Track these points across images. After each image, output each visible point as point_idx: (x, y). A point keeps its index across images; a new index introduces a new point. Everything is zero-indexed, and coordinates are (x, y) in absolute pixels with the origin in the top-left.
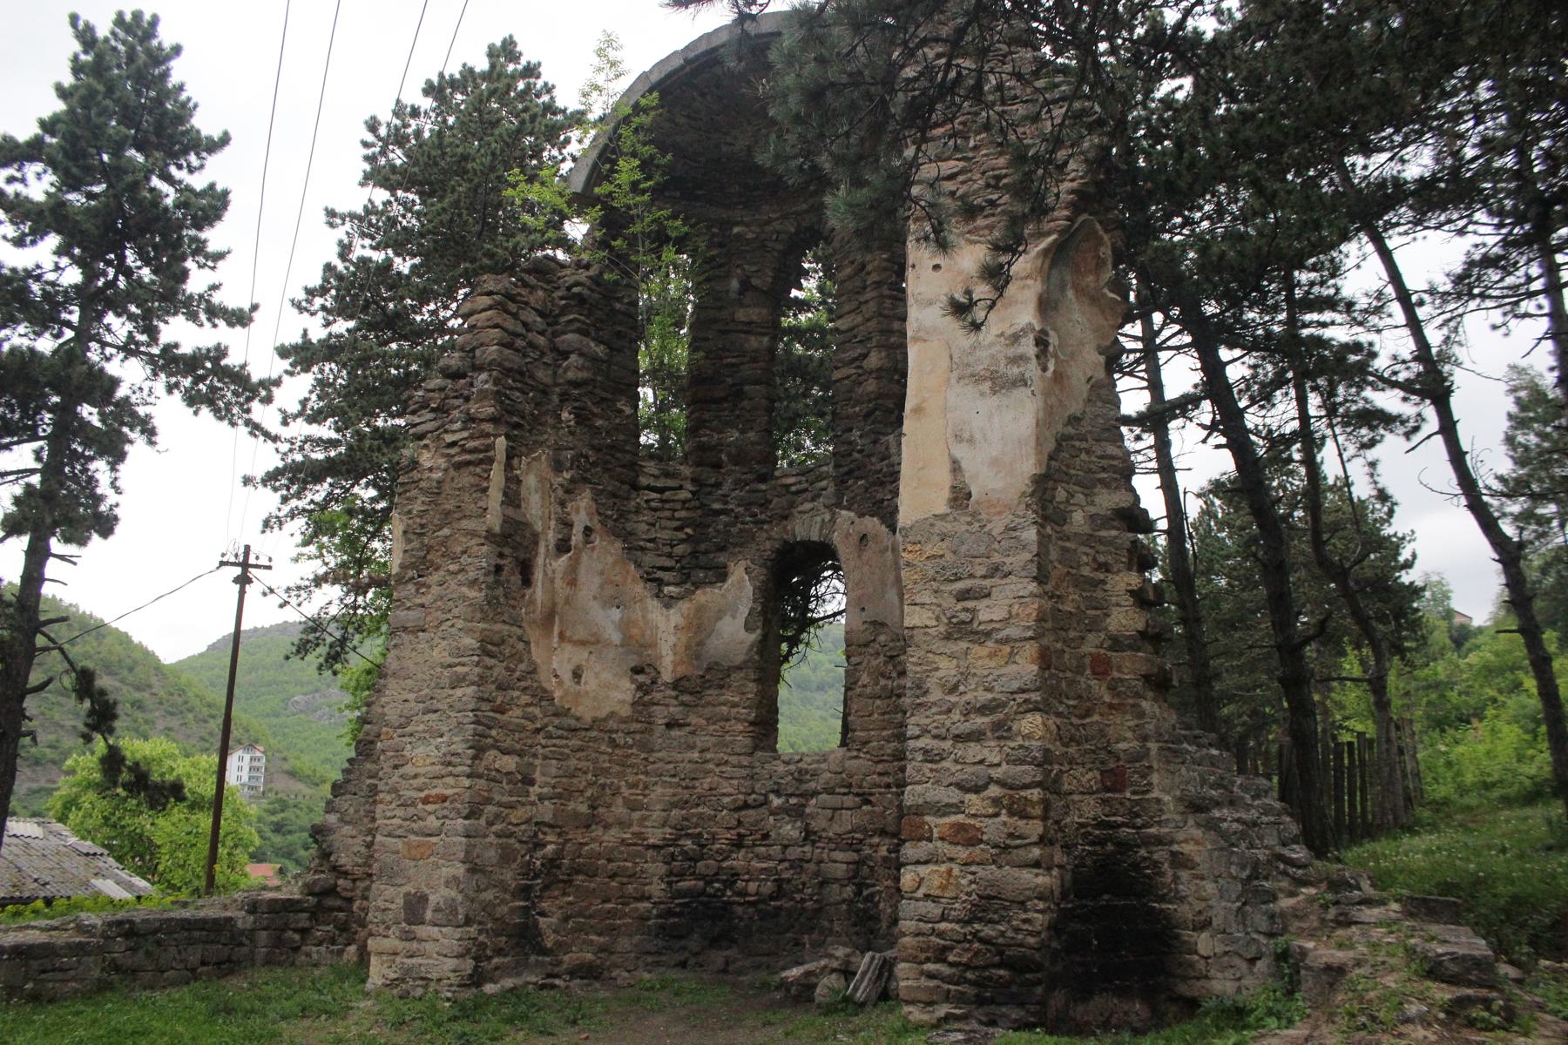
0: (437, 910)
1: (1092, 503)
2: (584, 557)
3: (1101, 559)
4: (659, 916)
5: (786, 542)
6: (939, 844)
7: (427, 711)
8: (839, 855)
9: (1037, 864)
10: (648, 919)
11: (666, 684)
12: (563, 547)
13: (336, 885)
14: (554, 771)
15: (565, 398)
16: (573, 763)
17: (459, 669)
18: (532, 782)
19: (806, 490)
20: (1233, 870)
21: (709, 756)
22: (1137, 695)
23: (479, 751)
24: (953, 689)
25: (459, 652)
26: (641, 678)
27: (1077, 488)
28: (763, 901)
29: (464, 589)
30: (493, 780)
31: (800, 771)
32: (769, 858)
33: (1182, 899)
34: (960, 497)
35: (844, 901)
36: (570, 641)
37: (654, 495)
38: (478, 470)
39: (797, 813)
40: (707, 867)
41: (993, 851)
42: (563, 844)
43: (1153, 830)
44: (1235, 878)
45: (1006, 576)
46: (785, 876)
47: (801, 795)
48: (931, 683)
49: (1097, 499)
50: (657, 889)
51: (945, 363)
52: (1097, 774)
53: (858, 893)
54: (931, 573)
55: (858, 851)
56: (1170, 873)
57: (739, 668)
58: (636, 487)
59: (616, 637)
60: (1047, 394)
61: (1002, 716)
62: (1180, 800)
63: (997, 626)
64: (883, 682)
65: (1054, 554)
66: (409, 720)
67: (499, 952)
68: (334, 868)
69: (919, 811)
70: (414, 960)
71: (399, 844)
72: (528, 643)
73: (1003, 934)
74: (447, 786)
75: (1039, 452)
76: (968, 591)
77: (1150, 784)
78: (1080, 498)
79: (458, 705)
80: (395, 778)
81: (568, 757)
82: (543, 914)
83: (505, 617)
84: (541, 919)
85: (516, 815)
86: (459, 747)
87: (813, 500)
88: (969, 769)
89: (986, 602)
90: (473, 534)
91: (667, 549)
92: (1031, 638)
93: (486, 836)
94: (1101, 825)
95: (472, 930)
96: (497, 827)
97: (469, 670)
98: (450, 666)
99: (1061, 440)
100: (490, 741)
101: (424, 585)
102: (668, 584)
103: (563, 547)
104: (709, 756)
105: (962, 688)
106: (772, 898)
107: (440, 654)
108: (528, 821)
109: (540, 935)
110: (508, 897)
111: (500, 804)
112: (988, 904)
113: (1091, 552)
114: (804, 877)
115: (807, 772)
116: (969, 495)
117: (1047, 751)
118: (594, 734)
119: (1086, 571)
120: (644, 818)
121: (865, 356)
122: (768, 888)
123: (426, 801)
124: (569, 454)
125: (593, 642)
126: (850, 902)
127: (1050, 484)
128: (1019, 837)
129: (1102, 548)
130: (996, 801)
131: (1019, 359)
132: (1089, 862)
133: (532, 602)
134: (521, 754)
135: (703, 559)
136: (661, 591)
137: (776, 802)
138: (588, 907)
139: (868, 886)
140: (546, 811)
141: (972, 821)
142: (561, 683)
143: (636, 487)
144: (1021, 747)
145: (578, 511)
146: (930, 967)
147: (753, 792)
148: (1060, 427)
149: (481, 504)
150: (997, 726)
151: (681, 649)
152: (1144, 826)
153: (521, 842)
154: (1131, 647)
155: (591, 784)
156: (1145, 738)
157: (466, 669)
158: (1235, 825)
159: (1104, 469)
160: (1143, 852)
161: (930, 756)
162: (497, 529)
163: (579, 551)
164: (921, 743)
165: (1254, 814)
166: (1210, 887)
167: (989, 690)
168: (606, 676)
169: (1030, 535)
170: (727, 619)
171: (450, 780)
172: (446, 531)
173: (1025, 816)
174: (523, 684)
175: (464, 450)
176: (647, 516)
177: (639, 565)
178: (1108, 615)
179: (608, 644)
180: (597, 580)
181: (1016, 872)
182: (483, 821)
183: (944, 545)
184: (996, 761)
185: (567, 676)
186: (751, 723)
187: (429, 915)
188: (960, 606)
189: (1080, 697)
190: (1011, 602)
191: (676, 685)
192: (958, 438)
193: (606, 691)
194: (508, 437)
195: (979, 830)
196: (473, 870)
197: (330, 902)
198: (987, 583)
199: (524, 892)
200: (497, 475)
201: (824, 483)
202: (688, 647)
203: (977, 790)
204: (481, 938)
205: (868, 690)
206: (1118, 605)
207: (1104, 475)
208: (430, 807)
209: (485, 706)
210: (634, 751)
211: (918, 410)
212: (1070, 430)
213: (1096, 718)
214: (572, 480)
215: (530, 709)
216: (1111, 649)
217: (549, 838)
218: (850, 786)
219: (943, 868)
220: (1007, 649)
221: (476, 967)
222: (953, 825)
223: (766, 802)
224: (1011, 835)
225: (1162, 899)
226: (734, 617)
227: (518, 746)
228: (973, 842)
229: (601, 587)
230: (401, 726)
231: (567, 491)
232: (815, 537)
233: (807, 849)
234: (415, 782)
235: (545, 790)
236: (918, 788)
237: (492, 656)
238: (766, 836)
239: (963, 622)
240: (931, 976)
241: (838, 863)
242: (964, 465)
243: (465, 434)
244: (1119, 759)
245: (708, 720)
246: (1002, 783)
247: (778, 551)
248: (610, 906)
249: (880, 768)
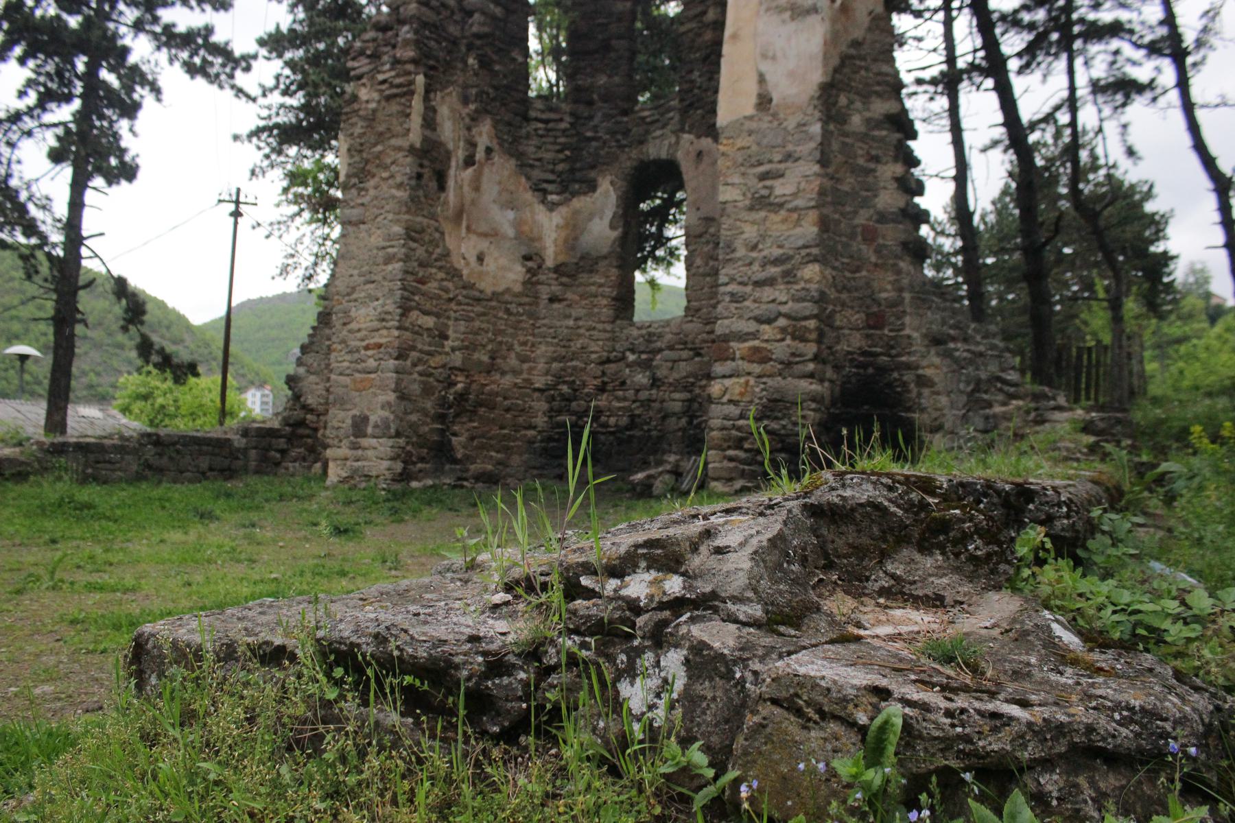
0: (376, 426)
1: (868, 110)
2: (486, 170)
3: (874, 152)
4: (542, 441)
5: (642, 162)
6: (740, 362)
8: (677, 396)
9: (811, 375)
10: (534, 443)
11: (549, 269)
12: (469, 161)
13: (305, 419)
14: (462, 329)
15: (470, 47)
16: (477, 324)
17: (390, 250)
18: (446, 338)
19: (657, 121)
20: (962, 386)
21: (581, 323)
22: (897, 257)
23: (405, 311)
24: (754, 248)
25: (389, 238)
26: (530, 264)
27: (856, 97)
29: (394, 191)
30: (416, 333)
31: (650, 334)
32: (625, 399)
33: (923, 410)
34: (764, 101)
35: (680, 429)
36: (475, 232)
37: (540, 125)
38: (403, 100)
39: (646, 365)
40: (579, 406)
41: (780, 366)
42: (470, 384)
43: (904, 359)
44: (962, 392)
45: (797, 160)
46: (637, 412)
47: (649, 352)
48: (738, 244)
49: (873, 107)
50: (541, 421)
52: (863, 315)
53: (690, 423)
54: (740, 160)
55: (690, 391)
56: (915, 391)
57: (605, 257)
58: (527, 119)
59: (511, 232)
60: (834, 21)
61: (789, 266)
62: (925, 336)
63: (789, 198)
64: (711, 263)
65: (835, 146)
66: (354, 289)
67: (422, 460)
69: (726, 338)
70: (359, 463)
71: (347, 380)
72: (442, 234)
73: (784, 427)
74: (381, 336)
75: (825, 65)
76: (768, 173)
77: (903, 324)
78: (858, 105)
79: (389, 277)
80: (345, 333)
81: (473, 320)
82: (455, 434)
83: (425, 213)
84: (454, 439)
85: (435, 361)
87: (663, 127)
88: (764, 307)
89: (781, 180)
90: (400, 149)
91: (551, 167)
92: (813, 207)
93: (411, 374)
94: (864, 353)
95: (402, 441)
96: (420, 368)
97: (397, 250)
98: (384, 248)
99: (845, 59)
100: (413, 304)
101: (363, 189)
102: (552, 193)
103: (469, 161)
104: (581, 323)
105: (760, 246)
106: (627, 428)
107: (376, 240)
108: (444, 366)
109: (453, 449)
110: (428, 420)
111: (421, 351)
113: (866, 147)
115: (654, 334)
116: (771, 100)
117: (822, 293)
118: (494, 303)
119: (861, 161)
120: (531, 369)
121: (704, 13)
122: (625, 421)
123: (367, 348)
124: (474, 91)
125: (492, 235)
126: (684, 430)
127: (834, 92)
128: (799, 356)
129: (875, 145)
130: (783, 330)
132: (853, 380)
133: (446, 203)
134: (438, 316)
135: (578, 175)
136: (545, 198)
137: (631, 357)
138: (488, 432)
139: (697, 417)
140: (457, 359)
141: (764, 345)
142: (468, 264)
143: (527, 119)
144: (803, 289)
145: (480, 134)
146: (731, 453)
147: (614, 350)
148: (844, 48)
149: (406, 126)
150: (786, 274)
151: (560, 242)
152: (899, 355)
153: (438, 381)
154: (894, 221)
155: (491, 341)
156: (901, 290)
157: (395, 250)
158: (965, 354)
159: (879, 84)
160: (896, 375)
161: (736, 298)
162: (418, 145)
163: (482, 165)
164: (729, 288)
165: (981, 348)
166: (944, 400)
167: (780, 247)
168: (503, 261)
169: (816, 128)
170: (596, 220)
171: (384, 332)
172: (379, 148)
173: (803, 339)
174: (439, 264)
175: (392, 86)
176: (535, 141)
177: (528, 178)
178: (876, 196)
179: (504, 237)
180: (496, 188)
181: (796, 382)
182: (409, 363)
183: (751, 139)
184: (784, 299)
185: (473, 260)
186: (614, 299)
187: (370, 430)
188: (761, 185)
189: (851, 257)
190: (799, 180)
191: (558, 269)
192: (764, 56)
193: (502, 272)
194: (426, 76)
195: (770, 351)
196: (403, 397)
197: (301, 431)
198: (782, 166)
199: (441, 418)
200: (417, 103)
201: (671, 114)
202: (566, 241)
203: (769, 321)
204: (409, 448)
205: (701, 270)
206: (885, 188)
207: (878, 88)
208: (370, 353)
209: (410, 278)
210: (524, 318)
211: (734, 37)
212: (853, 51)
213: (864, 273)
214: (476, 111)
215: (445, 283)
216: (878, 221)
217: (459, 379)
218: (685, 343)
219: (742, 380)
220: (795, 216)
221: (404, 469)
222: (750, 348)
223: (624, 358)
224: (793, 354)
225: (909, 409)
226: (601, 218)
227: (435, 310)
228: (765, 360)
229: (500, 193)
230: (348, 294)
231: (473, 119)
233: (654, 392)
234: (359, 335)
235: (456, 344)
236: (726, 322)
237: (414, 240)
238: (623, 383)
239: (763, 197)
240: (731, 459)
241: (676, 401)
242: (768, 77)
243: (393, 73)
244: (880, 305)
245: (581, 296)
247: (636, 168)
248: (506, 431)
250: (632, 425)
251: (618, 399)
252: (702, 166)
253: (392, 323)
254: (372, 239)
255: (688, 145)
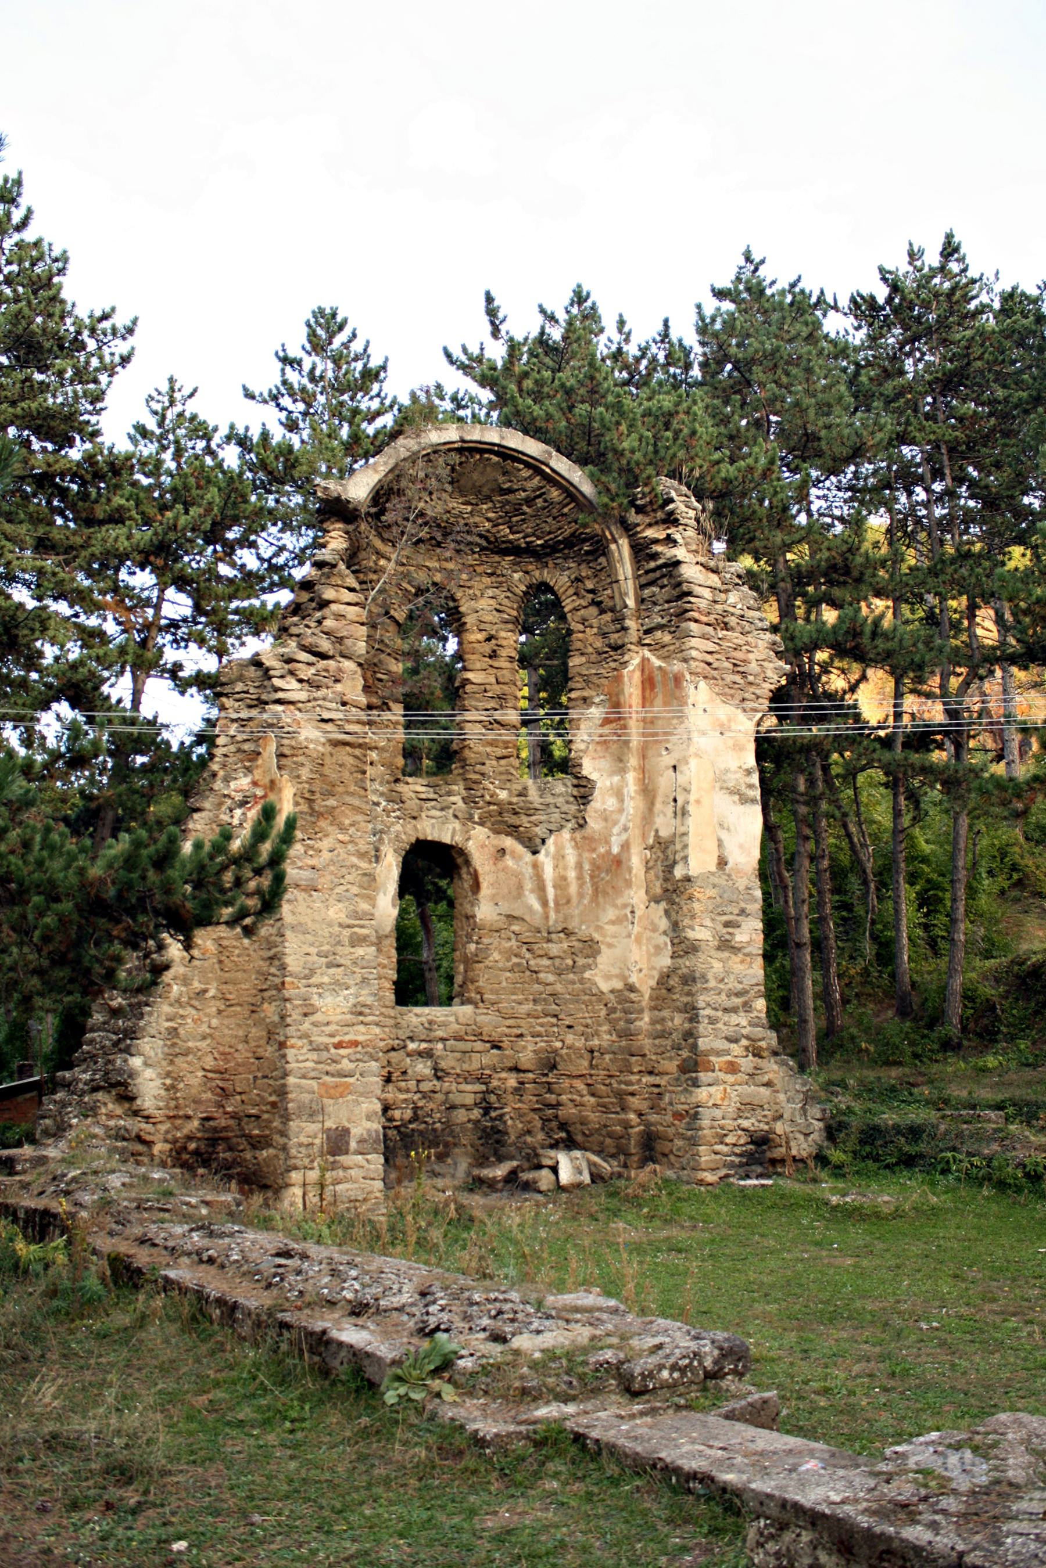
7: (330, 965)
8: (469, 1087)
25: (356, 915)
28: (404, 1125)
29: (354, 860)
31: (430, 1022)
32: (408, 1091)
34: (722, 863)
38: (358, 752)
39: (428, 1054)
48: (710, 976)
51: (711, 775)
64: (515, 960)
66: (313, 972)
68: (136, 1113)
74: (357, 1033)
80: (306, 1026)
86: (369, 1000)
107: (337, 912)
112: (748, 1106)
114: (431, 1105)
122: (408, 1114)
123: (338, 1046)
130: (747, 1048)
131: (751, 786)
137: (412, 1046)
146: (718, 1147)
150: (745, 1004)
161: (712, 1021)
164: (708, 1012)
166: (782, 1097)
169: (758, 894)
171: (362, 1028)
172: (332, 802)
187: (353, 1145)
201: (453, 799)
203: (736, 1041)
208: (342, 1052)
211: (698, 802)
230: (306, 977)
232: (447, 840)
234: (328, 1029)
238: (404, 1073)
241: (468, 1093)
243: (341, 716)
246: (748, 1038)
249: (510, 1022)
250: (415, 1118)
251: (400, 1090)
252: (500, 865)
253: (370, 1018)
254: (332, 913)
255: (482, 837)
